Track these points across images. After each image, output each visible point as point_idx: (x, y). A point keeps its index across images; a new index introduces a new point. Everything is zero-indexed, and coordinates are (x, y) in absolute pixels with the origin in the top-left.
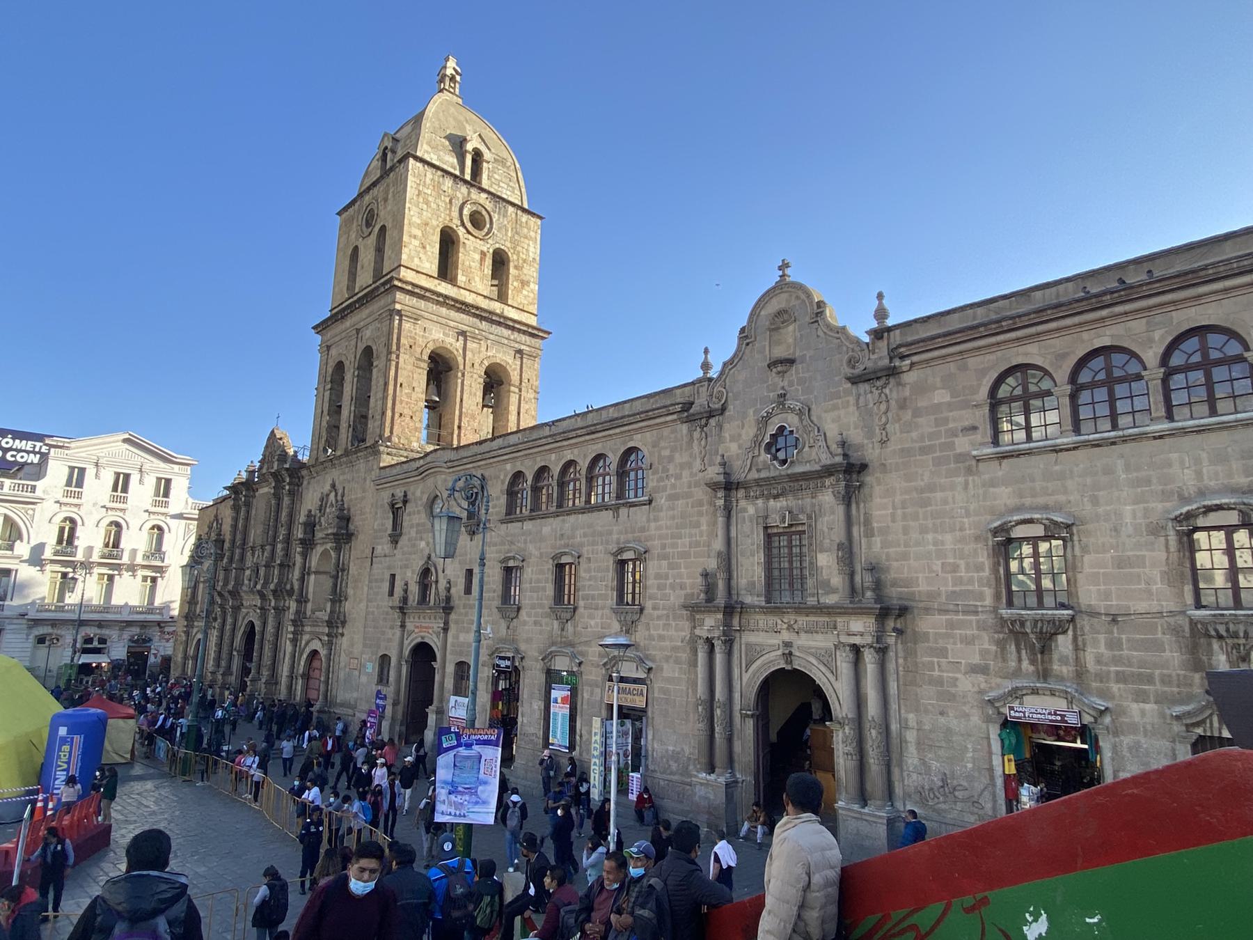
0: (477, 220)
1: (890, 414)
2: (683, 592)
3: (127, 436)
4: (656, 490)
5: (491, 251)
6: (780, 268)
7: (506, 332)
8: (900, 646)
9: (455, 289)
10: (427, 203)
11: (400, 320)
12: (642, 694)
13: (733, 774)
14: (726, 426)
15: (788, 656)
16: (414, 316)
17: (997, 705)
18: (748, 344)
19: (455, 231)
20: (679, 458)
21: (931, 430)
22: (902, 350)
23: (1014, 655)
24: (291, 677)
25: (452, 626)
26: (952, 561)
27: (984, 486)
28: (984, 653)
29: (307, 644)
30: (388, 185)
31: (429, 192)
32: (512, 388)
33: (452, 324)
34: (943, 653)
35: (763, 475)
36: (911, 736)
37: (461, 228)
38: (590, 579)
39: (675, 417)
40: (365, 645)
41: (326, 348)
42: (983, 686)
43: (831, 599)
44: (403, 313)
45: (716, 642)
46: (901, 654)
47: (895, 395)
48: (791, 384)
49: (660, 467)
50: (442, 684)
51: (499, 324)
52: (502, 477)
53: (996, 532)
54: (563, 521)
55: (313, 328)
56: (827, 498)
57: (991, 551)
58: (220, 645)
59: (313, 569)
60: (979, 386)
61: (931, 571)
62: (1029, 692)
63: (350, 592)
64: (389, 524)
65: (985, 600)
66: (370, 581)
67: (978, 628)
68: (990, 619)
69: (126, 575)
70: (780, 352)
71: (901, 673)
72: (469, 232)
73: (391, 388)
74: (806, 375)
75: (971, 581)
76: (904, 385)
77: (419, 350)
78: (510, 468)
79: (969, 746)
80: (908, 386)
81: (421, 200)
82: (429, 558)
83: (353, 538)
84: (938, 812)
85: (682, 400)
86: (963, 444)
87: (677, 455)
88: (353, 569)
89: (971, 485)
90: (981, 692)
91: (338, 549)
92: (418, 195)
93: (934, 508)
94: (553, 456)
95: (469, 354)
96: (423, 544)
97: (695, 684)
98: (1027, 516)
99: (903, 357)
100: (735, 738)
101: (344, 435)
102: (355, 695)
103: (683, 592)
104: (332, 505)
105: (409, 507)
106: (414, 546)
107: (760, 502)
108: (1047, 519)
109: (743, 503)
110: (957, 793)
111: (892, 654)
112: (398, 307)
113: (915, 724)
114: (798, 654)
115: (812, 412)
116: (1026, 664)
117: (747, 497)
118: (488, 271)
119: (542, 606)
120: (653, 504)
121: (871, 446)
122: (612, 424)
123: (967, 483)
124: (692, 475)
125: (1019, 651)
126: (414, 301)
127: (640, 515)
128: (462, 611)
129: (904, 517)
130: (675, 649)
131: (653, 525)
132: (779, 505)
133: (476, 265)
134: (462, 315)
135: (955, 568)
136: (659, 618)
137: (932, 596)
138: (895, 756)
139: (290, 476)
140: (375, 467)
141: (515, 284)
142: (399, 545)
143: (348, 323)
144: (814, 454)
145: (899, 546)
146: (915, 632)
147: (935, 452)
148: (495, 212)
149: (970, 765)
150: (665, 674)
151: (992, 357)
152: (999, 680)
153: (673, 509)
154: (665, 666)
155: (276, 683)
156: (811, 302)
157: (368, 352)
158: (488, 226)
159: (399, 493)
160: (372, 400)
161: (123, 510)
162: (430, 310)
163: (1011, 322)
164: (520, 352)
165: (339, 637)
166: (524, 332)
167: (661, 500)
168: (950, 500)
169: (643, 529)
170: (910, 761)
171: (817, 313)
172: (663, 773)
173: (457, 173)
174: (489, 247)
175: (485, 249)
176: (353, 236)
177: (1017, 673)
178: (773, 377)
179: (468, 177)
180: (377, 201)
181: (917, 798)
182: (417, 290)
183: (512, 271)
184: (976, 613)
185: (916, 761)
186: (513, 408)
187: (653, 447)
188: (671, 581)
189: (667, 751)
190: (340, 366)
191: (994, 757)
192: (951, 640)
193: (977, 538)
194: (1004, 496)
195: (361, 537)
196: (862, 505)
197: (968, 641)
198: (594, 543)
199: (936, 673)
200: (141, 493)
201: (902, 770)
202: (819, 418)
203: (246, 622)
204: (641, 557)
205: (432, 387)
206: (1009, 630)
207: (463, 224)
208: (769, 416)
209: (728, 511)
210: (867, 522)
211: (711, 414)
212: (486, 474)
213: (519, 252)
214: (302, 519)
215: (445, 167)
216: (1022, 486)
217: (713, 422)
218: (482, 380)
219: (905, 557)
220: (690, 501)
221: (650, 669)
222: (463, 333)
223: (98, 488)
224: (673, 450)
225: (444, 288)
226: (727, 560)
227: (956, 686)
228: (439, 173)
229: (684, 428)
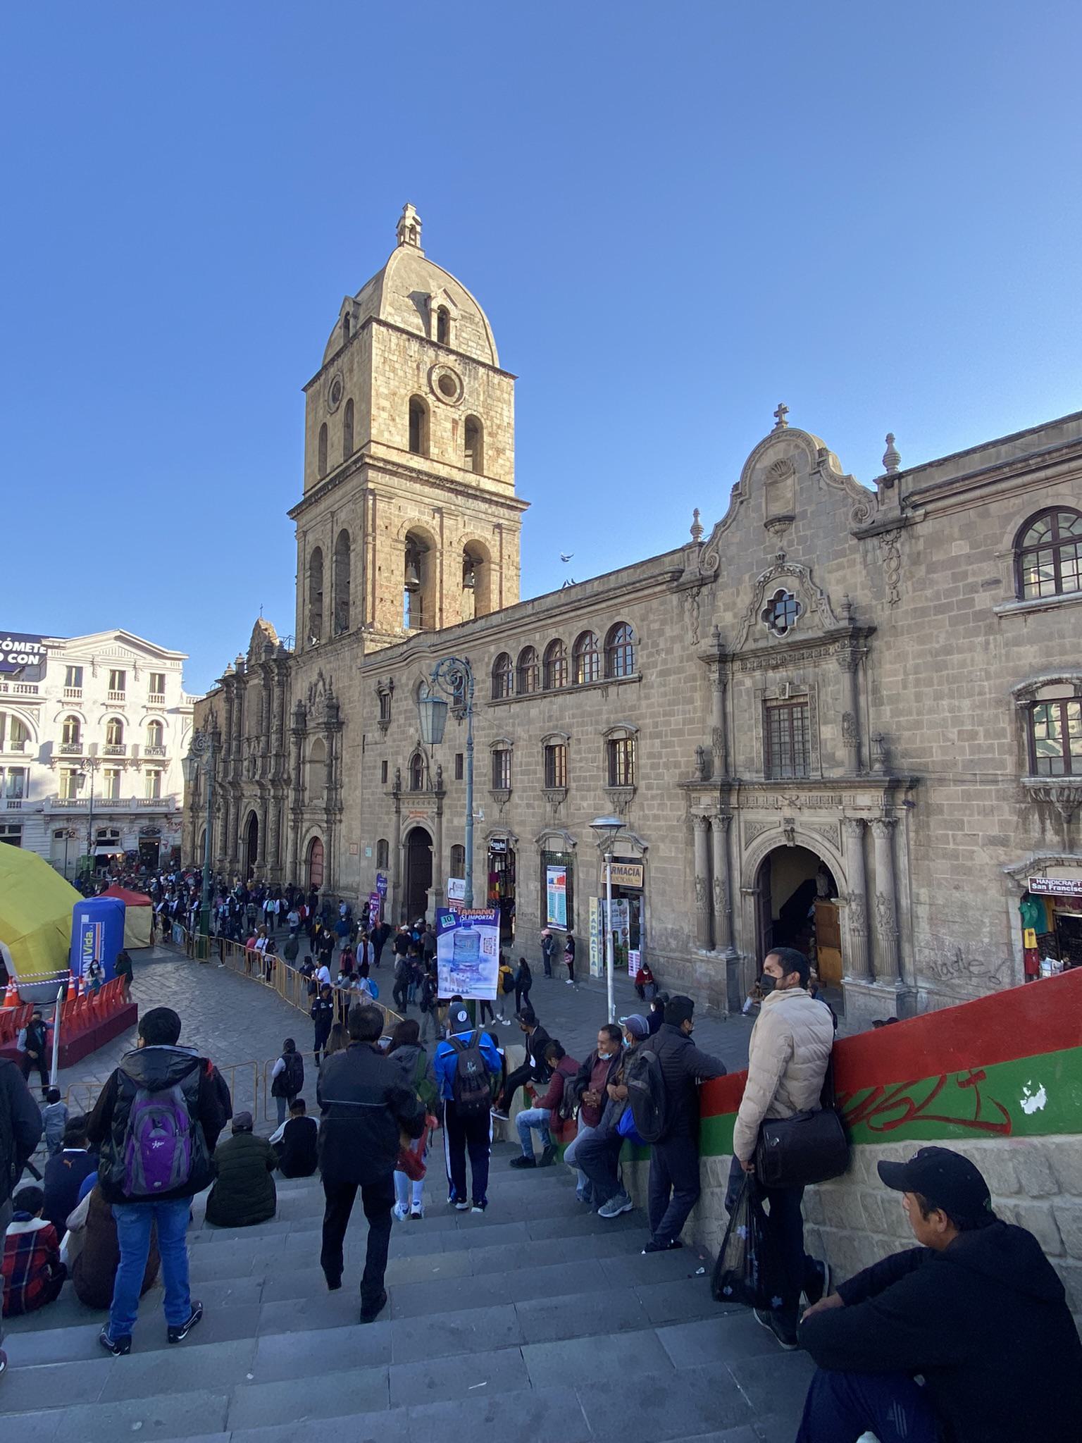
0: (447, 386)
1: (901, 571)
2: (677, 771)
3: (118, 634)
4: (647, 666)
5: (463, 418)
6: (776, 414)
7: (484, 506)
8: (911, 819)
9: (428, 462)
10: (394, 370)
11: (374, 500)
12: (638, 874)
13: (734, 951)
14: (720, 594)
15: (790, 833)
16: (388, 495)
17: (1017, 877)
18: (742, 502)
19: (424, 399)
20: (669, 631)
21: (946, 586)
22: (915, 498)
23: (1037, 825)
24: (295, 863)
25: (446, 811)
26: (970, 728)
27: (1006, 645)
28: (1003, 824)
29: (307, 831)
30: (352, 355)
31: (395, 358)
32: (493, 566)
33: (427, 500)
34: (959, 825)
35: (762, 644)
36: (923, 911)
37: (430, 395)
38: (581, 761)
39: (664, 587)
40: (363, 831)
41: (303, 534)
42: (1003, 858)
43: (835, 773)
44: (376, 492)
45: (713, 821)
46: (912, 828)
47: (907, 549)
48: (791, 544)
49: (650, 641)
50: (440, 866)
51: (475, 497)
52: (486, 659)
53: (1019, 695)
54: (551, 702)
55: (289, 513)
56: (830, 666)
57: (1013, 716)
58: (225, 834)
59: (307, 759)
60: (1003, 534)
61: (946, 739)
62: (1053, 863)
63: (345, 779)
65: (1006, 769)
66: (364, 769)
67: (998, 799)
68: (1011, 788)
69: (131, 769)
70: (778, 509)
71: (912, 847)
72: (439, 400)
73: (370, 572)
74: (808, 533)
75: (991, 748)
76: (918, 538)
77: (395, 531)
78: (494, 650)
79: (987, 920)
80: (922, 540)
81: (387, 368)
82: (419, 744)
83: (344, 727)
84: (952, 987)
85: (671, 569)
86: (983, 600)
87: (667, 628)
88: (346, 757)
89: (992, 646)
90: (1001, 865)
91: (330, 738)
92: (384, 363)
93: (951, 672)
94: (538, 636)
95: (446, 532)
96: (412, 730)
97: (692, 863)
98: (1056, 676)
99: (915, 507)
100: (736, 915)
101: (328, 624)
102: (357, 879)
103: (677, 771)
104: (321, 695)
106: (403, 732)
107: (758, 674)
108: (1078, 678)
109: (739, 676)
110: (972, 969)
111: (902, 828)
112: (371, 485)
113: (927, 899)
114: (800, 830)
115: (814, 573)
116: (1051, 836)
117: (744, 669)
118: (461, 441)
119: (533, 789)
120: (644, 681)
121: (879, 607)
122: (597, 599)
123: (987, 643)
124: (684, 649)
125: (1042, 821)
126: (387, 478)
127: (630, 692)
128: (455, 795)
129: (918, 683)
130: (671, 828)
131: (644, 703)
132: (778, 676)
133: (448, 434)
134: (440, 492)
135: (973, 735)
136: (653, 798)
137: (946, 765)
138: (905, 932)
139: (278, 667)
140: (360, 654)
141: (490, 452)
142: (389, 732)
143: (323, 505)
144: (816, 619)
145: (910, 713)
146: (928, 805)
147: (952, 610)
148: (464, 374)
149: (986, 940)
150: (661, 854)
151: (1018, 501)
152: (1019, 852)
153: (665, 686)
154: (662, 846)
155: (281, 869)
156: (812, 451)
157: (344, 535)
158: (458, 391)
159: (385, 680)
160: (352, 586)
161: (122, 707)
162: (403, 487)
163: (1039, 459)
164: (498, 526)
165: (338, 824)
166: (502, 505)
167: (652, 676)
168: (968, 661)
169: (633, 708)
170: (922, 937)
171: (819, 463)
172: (664, 950)
173: (423, 334)
174: (460, 414)
175: (457, 417)
176: (321, 412)
177: (1041, 844)
178: (770, 537)
179: (434, 338)
180: (342, 372)
181: (928, 973)
182: (389, 467)
183: (486, 438)
184: (996, 782)
185: (929, 937)
186: (494, 587)
187: (643, 620)
188: (664, 760)
189: (666, 929)
190: (318, 551)
191: (1013, 931)
192: (968, 812)
193: (999, 703)
194: (1029, 655)
195: (351, 726)
196: (870, 672)
197: (987, 812)
198: (583, 724)
199: (951, 846)
200: (137, 689)
201: (913, 946)
202: (822, 579)
203: (247, 812)
204: (632, 736)
205: (412, 569)
206: (1033, 799)
207: (432, 392)
208: (767, 580)
209: (723, 685)
210: (876, 690)
211: (702, 582)
212: (471, 656)
213: (492, 417)
214: (293, 709)
215: (410, 329)
216: (1050, 644)
217: (705, 590)
218: (461, 560)
219: (917, 725)
220: (683, 676)
221: (645, 849)
222: (439, 510)
223: (96, 686)
224: (663, 622)
225: (416, 462)
226: (723, 736)
227: (972, 859)
228: (405, 336)
229: (675, 598)
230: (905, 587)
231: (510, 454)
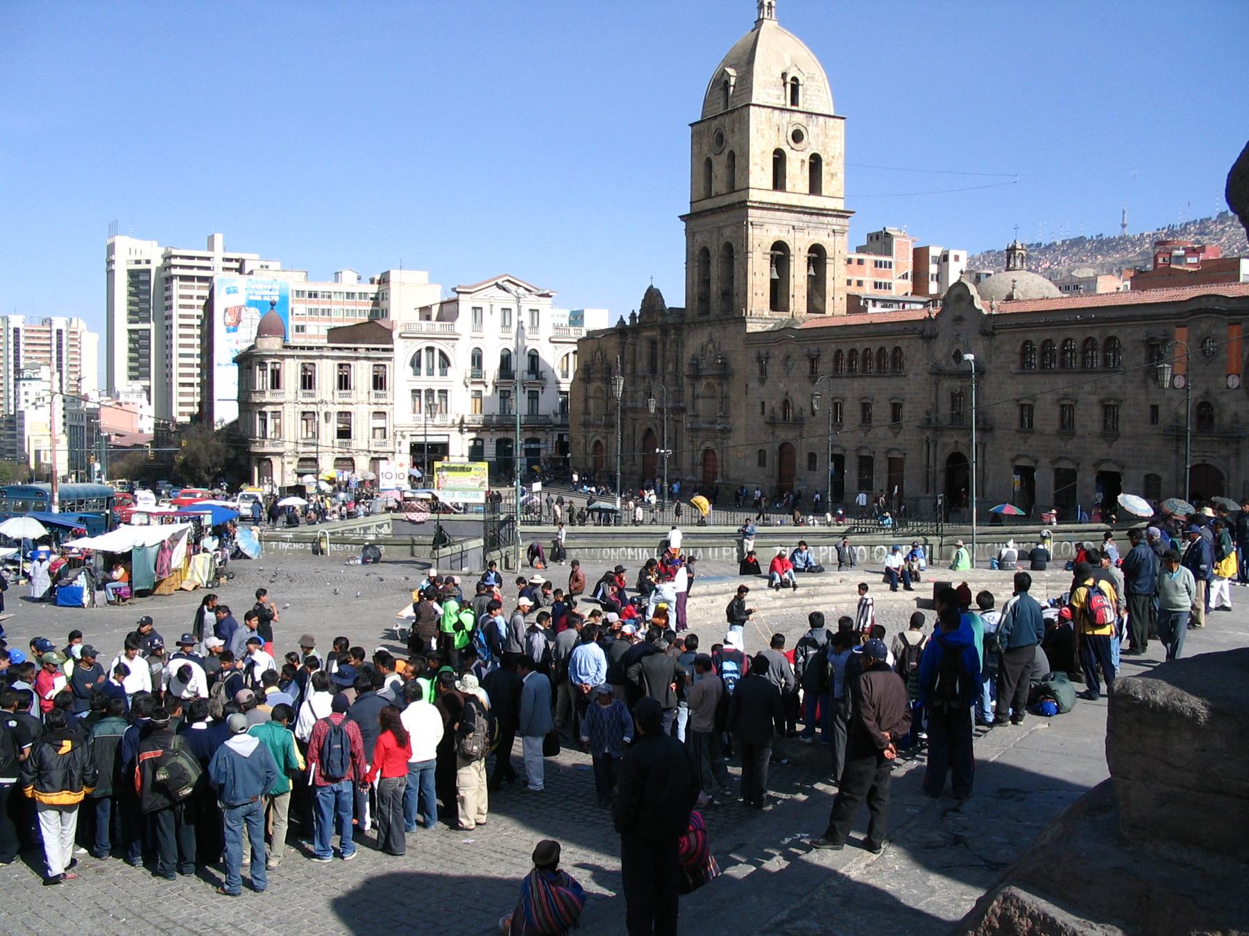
0: (797, 136)
10: (763, 136)
24: (693, 464)
33: (784, 222)
41: (690, 233)
55: (680, 217)
64: (757, 370)
70: (957, 313)
72: (792, 148)
88: (733, 396)
96: (782, 385)
105: (771, 361)
159: (763, 352)
167: (911, 376)
169: (902, 389)
176: (705, 149)
183: (825, 169)
190: (705, 252)
203: (644, 427)
228: (770, 110)
229: (921, 342)
230: (993, 357)
231: (841, 176)
